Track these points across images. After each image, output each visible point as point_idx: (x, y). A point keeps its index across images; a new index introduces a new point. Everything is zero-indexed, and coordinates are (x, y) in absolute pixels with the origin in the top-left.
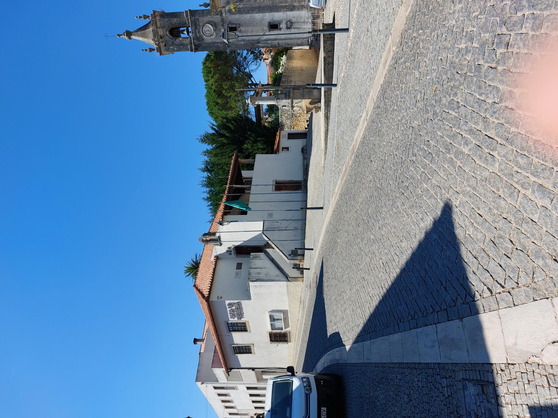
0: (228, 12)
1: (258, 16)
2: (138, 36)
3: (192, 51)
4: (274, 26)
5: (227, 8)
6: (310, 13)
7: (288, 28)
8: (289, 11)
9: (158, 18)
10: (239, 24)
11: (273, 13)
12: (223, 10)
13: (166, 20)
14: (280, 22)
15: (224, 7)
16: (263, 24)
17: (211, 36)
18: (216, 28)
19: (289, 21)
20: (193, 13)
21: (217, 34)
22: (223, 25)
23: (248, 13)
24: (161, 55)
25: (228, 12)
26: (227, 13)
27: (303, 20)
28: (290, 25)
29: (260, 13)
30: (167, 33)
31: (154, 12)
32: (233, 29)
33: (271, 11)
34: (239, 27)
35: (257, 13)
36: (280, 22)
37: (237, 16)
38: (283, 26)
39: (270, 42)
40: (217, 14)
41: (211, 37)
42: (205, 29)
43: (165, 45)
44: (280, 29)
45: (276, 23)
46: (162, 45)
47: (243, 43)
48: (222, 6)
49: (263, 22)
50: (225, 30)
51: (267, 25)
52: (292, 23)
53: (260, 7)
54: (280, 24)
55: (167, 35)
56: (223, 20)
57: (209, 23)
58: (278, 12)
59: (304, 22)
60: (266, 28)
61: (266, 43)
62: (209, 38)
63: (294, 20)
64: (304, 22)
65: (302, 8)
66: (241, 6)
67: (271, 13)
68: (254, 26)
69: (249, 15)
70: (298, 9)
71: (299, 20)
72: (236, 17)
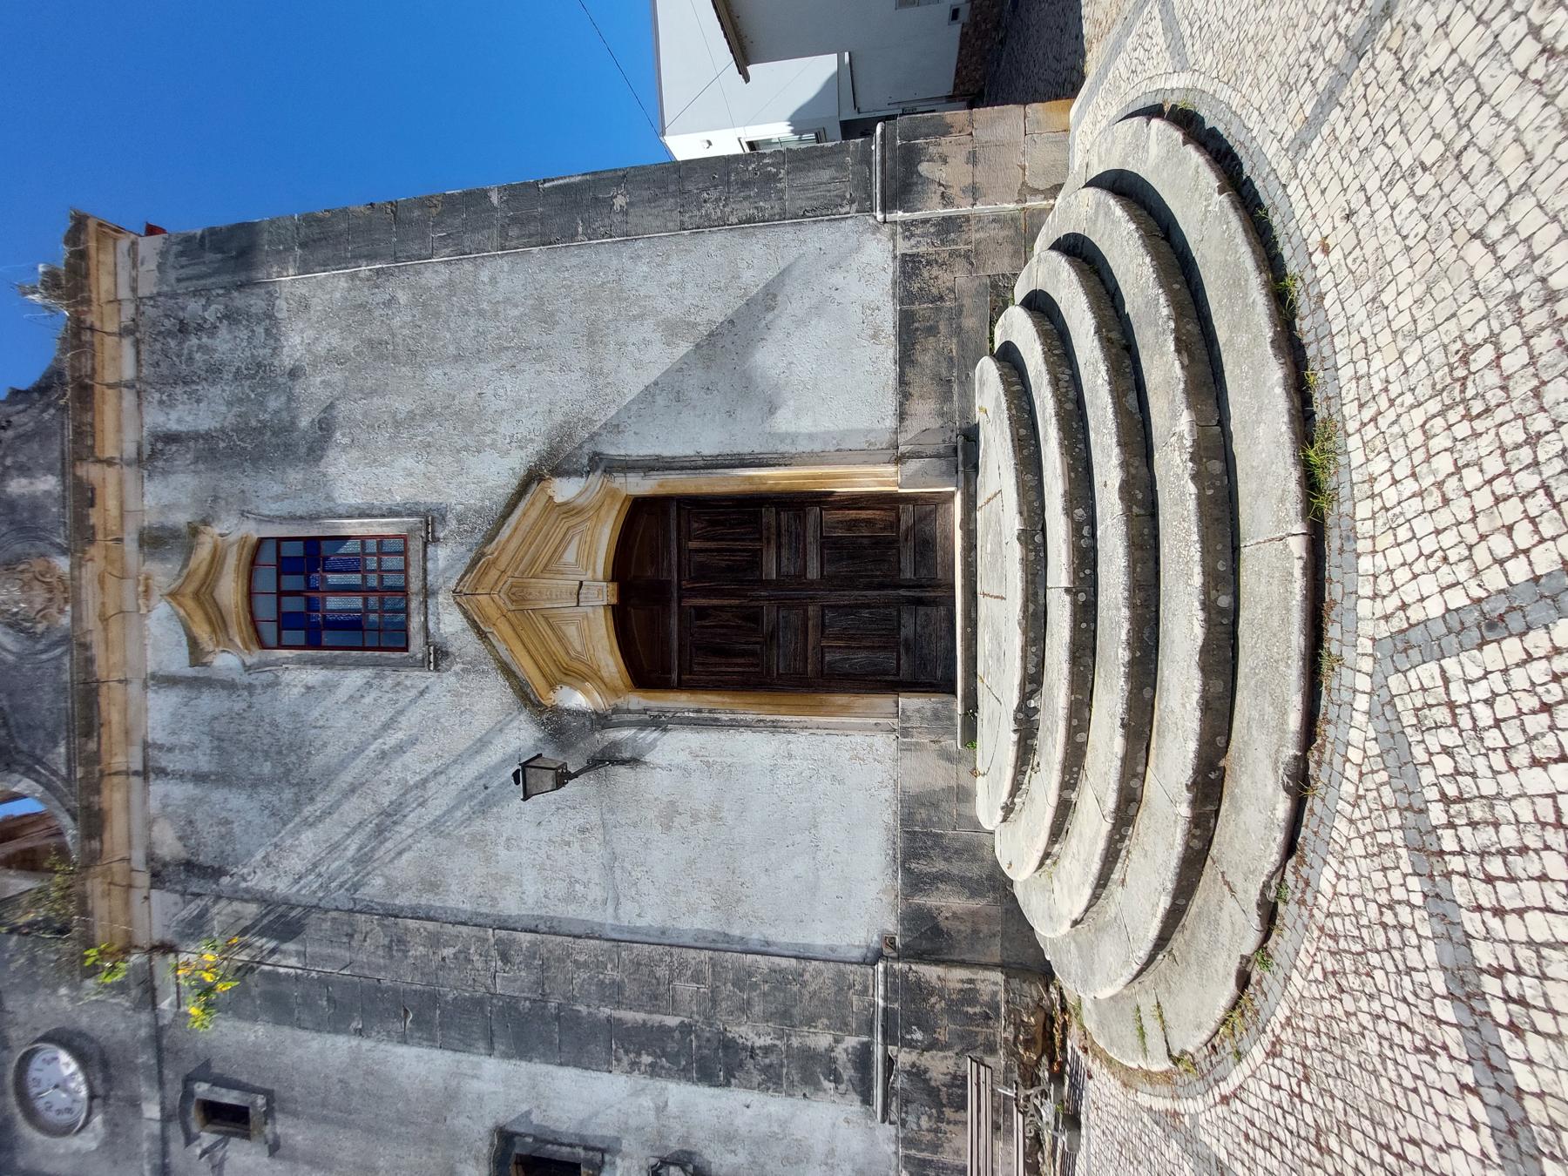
1: (415, 1064)
8: (683, 1074)
10: (269, 1095)
11: (538, 1068)
15: (166, 948)
16: (454, 1139)
17: (66, 1130)
18: (107, 1079)
21: (110, 1123)
23: (337, 1024)
29: (431, 1042)
33: (522, 1048)
34: (269, 1114)
35: (404, 1040)
48: (158, 935)
49: (460, 1122)
50: (166, 1119)
51: (485, 1149)
53: (434, 999)
57: (66, 1039)
66: (288, 962)
68: (374, 1131)
70: (772, 1080)
72: (241, 1040)
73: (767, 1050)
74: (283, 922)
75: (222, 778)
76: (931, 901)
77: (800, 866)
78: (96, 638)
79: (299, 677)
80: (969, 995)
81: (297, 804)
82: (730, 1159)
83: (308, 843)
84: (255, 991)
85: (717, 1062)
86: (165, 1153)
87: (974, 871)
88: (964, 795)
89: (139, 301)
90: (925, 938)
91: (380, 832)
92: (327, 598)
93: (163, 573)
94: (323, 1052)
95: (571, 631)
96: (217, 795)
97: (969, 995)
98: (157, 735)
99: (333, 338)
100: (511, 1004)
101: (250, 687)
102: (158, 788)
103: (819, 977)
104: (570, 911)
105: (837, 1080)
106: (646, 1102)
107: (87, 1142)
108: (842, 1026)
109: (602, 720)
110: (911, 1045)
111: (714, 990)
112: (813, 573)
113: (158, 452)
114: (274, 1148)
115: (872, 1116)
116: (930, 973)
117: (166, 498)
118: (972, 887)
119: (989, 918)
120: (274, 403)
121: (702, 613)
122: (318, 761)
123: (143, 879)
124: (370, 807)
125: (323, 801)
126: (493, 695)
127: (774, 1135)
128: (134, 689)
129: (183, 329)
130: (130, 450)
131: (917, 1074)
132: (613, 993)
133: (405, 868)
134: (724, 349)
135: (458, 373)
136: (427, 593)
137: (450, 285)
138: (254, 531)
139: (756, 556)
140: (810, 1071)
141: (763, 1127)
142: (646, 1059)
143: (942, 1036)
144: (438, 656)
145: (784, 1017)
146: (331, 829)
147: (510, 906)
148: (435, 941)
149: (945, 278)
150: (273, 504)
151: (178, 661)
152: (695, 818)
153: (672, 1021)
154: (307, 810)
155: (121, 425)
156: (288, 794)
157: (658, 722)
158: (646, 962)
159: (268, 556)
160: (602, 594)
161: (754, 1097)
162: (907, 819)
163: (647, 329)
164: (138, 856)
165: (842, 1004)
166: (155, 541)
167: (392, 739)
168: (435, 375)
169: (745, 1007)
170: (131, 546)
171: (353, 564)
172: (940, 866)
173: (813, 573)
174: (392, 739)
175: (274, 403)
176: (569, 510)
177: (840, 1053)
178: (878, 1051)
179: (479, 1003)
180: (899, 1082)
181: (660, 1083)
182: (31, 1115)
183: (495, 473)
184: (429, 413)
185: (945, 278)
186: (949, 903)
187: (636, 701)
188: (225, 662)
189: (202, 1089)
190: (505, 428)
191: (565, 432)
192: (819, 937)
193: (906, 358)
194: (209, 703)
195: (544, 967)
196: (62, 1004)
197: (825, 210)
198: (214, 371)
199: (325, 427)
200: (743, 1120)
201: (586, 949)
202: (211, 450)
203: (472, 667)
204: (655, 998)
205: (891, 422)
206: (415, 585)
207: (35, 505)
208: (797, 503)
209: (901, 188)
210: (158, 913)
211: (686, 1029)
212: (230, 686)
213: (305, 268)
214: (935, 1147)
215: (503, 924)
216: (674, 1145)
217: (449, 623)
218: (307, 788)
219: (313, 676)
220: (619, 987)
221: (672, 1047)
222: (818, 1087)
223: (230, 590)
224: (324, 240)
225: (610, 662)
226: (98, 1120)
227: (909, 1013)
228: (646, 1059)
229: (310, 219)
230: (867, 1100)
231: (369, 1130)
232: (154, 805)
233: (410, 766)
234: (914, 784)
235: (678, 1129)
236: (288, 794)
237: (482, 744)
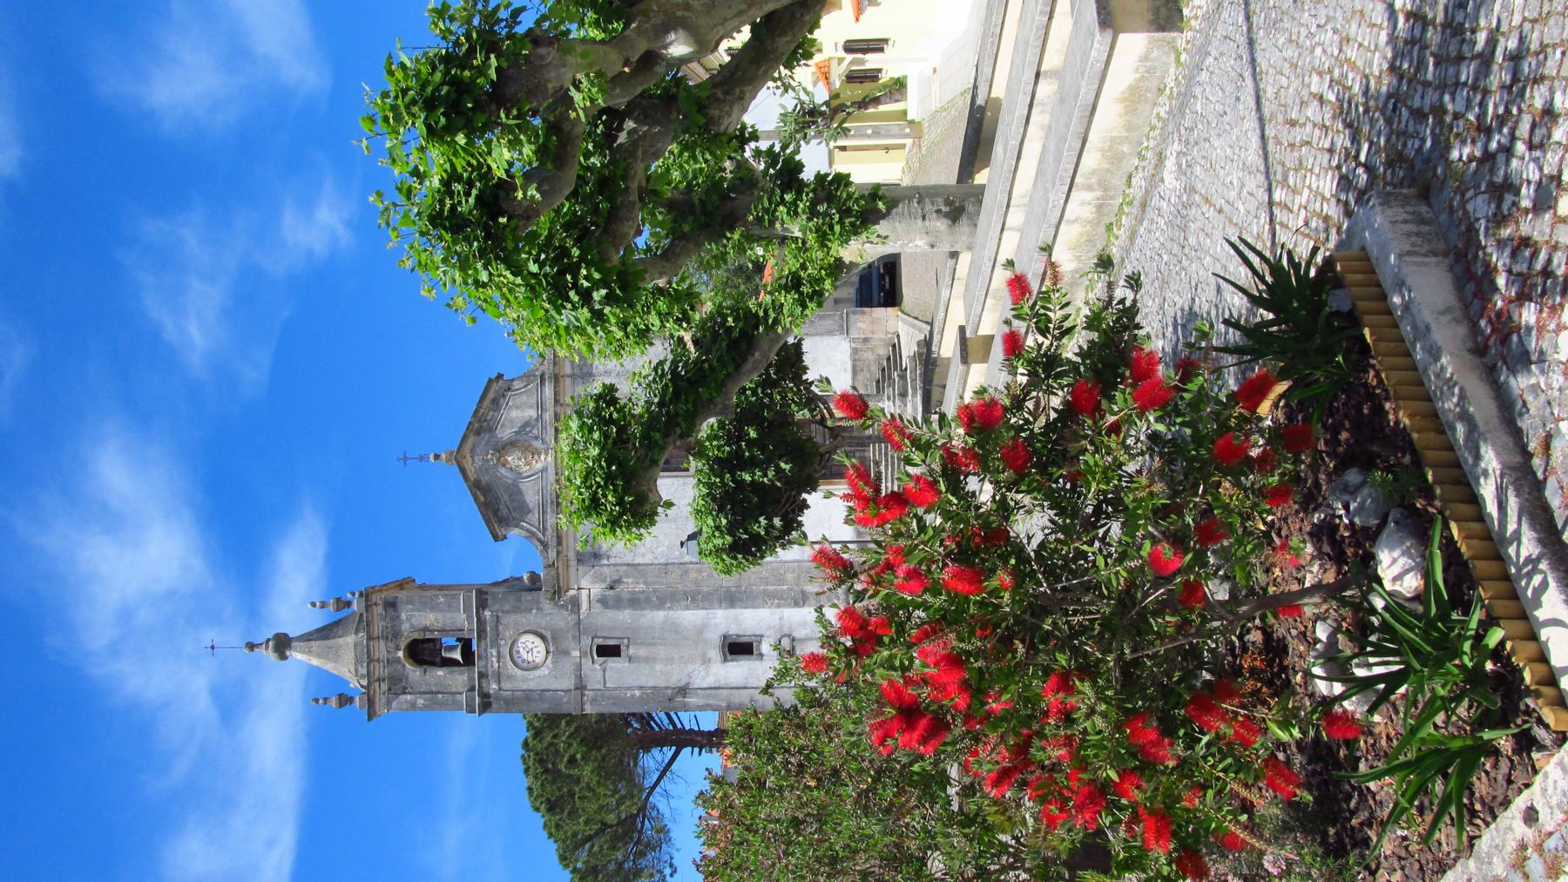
0: (599, 601)
1: (690, 617)
2: (310, 652)
3: (471, 710)
8: (789, 606)
17: (536, 667)
20: (483, 597)
23: (660, 605)
25: (599, 601)
29: (697, 607)
30: (401, 654)
35: (687, 608)
37: (625, 616)
41: (537, 673)
44: (761, 655)
45: (744, 640)
58: (753, 607)
60: (715, 654)
62: (532, 674)
63: (797, 634)
67: (732, 612)
94: (656, 617)
100: (728, 591)
106: (777, 617)
107: (545, 671)
114: (630, 659)
123: (573, 563)
164: (572, 555)
189: (600, 641)
196: (532, 619)
197: (830, 333)
204: (781, 581)
216: (786, 631)
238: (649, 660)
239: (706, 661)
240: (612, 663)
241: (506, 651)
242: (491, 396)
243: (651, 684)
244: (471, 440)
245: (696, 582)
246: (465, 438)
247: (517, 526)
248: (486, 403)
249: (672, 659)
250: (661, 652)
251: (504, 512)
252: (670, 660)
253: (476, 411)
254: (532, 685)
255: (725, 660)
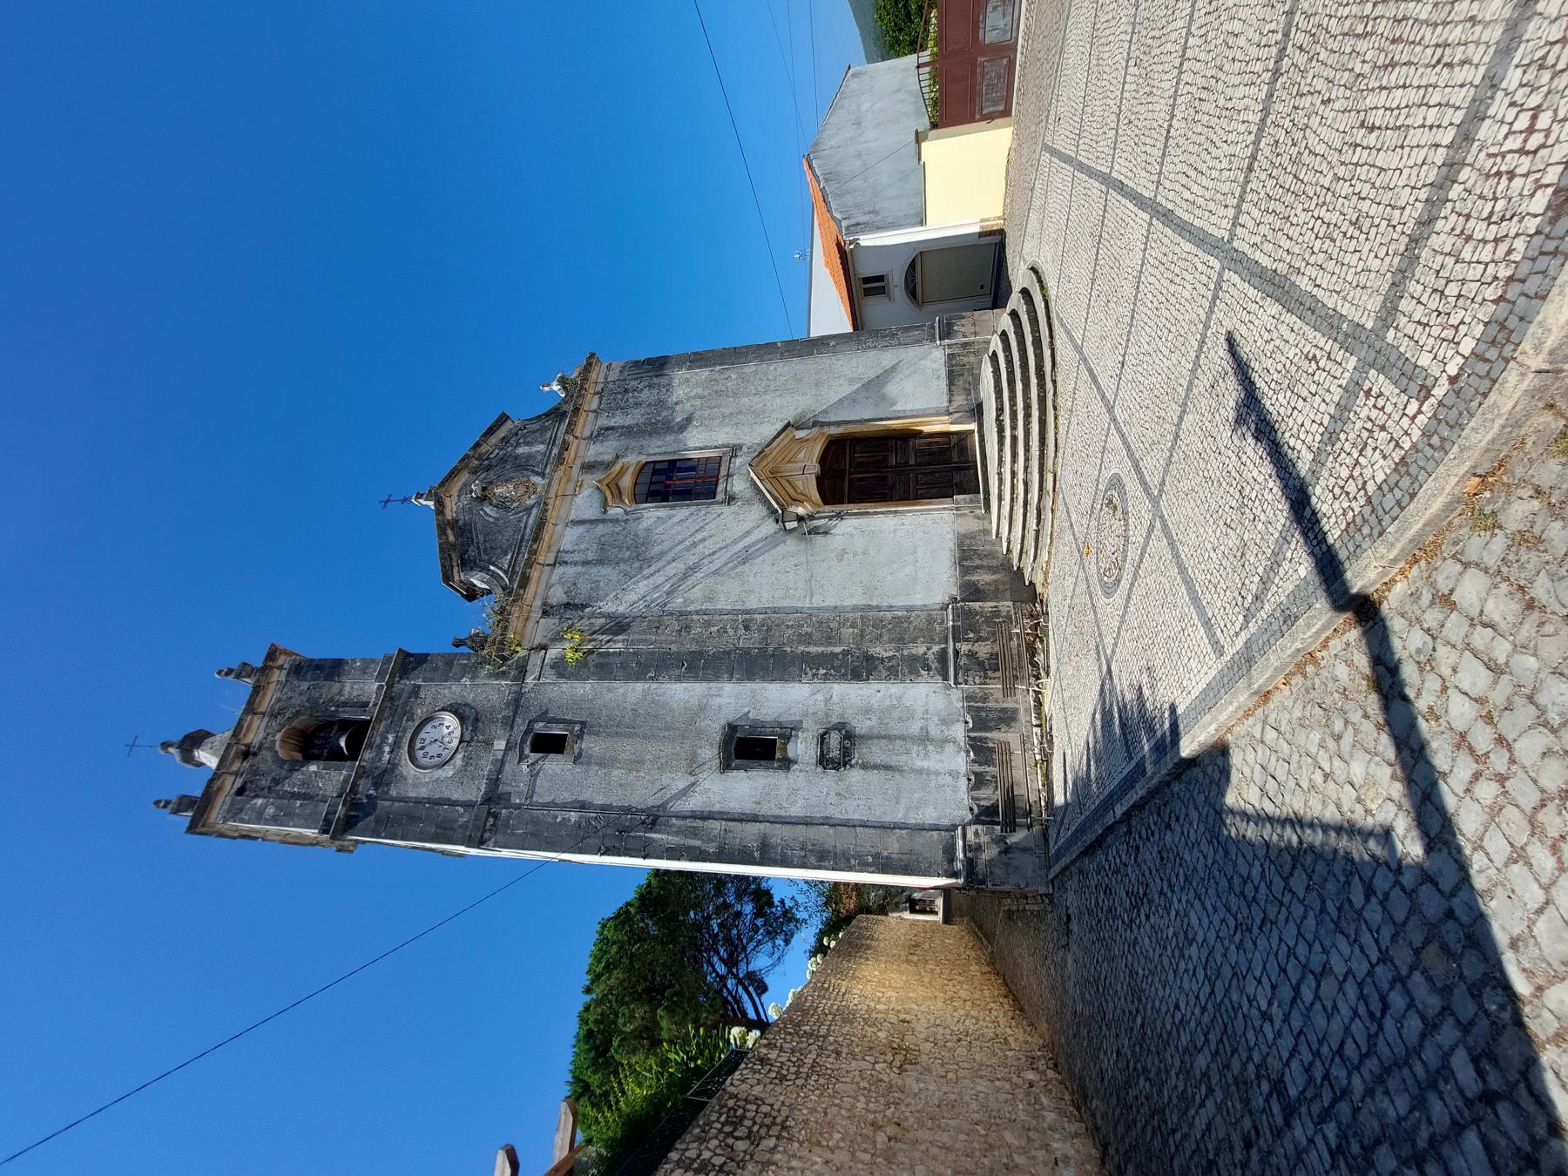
1: (680, 693)
4: (752, 747)
5: (553, 653)
6: (956, 694)
7: (824, 761)
8: (843, 678)
9: (278, 676)
10: (583, 724)
12: (536, 659)
13: (305, 685)
14: (788, 732)
16: (700, 733)
18: (475, 730)
19: (840, 727)
20: (408, 663)
21: (468, 760)
22: (510, 723)
23: (639, 676)
24: (192, 828)
25: (552, 667)
26: (548, 671)
27: (915, 728)
28: (841, 749)
29: (697, 679)
30: (278, 736)
31: (272, 654)
32: (549, 745)
33: (749, 676)
34: (580, 736)
35: (679, 679)
36: (788, 732)
38: (803, 748)
39: (716, 826)
40: (504, 675)
41: (440, 773)
42: (428, 733)
43: (241, 791)
44: (787, 764)
46: (230, 784)
47: (573, 816)
49: (703, 724)
50: (508, 748)
51: (717, 738)
52: (849, 736)
54: (788, 738)
55: (271, 748)
56: (517, 702)
57: (455, 710)
58: (781, 679)
59: (924, 739)
60: (709, 753)
61: (694, 833)
62: (426, 776)
63: (861, 726)
64: (924, 739)
65: (914, 672)
66: (618, 646)
69: (639, 687)
70: (893, 674)
71: (896, 728)
73: (890, 658)
74: (618, 626)
75: (600, 562)
76: (974, 578)
77: (907, 570)
78: (551, 502)
79: (652, 514)
80: (996, 613)
81: (641, 569)
82: (868, 723)
83: (643, 587)
84: (591, 664)
85: (861, 668)
86: (500, 771)
87: (995, 563)
88: (987, 532)
89: (606, 382)
90: (972, 592)
91: (685, 577)
92: (680, 482)
93: (591, 480)
94: (633, 691)
95: (799, 483)
96: (594, 570)
97: (996, 613)
98: (568, 547)
99: (700, 391)
100: (747, 651)
101: (626, 521)
102: (559, 570)
103: (919, 620)
104: (786, 603)
105: (929, 669)
106: (820, 697)
107: (448, 771)
108: (932, 641)
109: (811, 517)
110: (967, 640)
111: (862, 631)
112: (912, 462)
113: (601, 434)
114: (577, 759)
115: (949, 687)
116: (976, 605)
117: (602, 451)
118: (994, 570)
119: (1003, 583)
120: (664, 413)
121: (860, 480)
122: (656, 549)
123: (537, 614)
124: (682, 566)
125: (653, 568)
126: (757, 511)
127: (893, 706)
128: (559, 528)
129: (626, 391)
130: (587, 433)
131: (972, 655)
132: (807, 639)
133: (697, 593)
134: (875, 386)
135: (756, 399)
136: (729, 475)
137: (756, 372)
138: (644, 459)
139: (885, 459)
140: (913, 667)
141: (888, 703)
142: (822, 671)
143: (983, 634)
144: (731, 499)
145: (900, 640)
146: (659, 578)
147: (753, 603)
148: (708, 624)
149: (965, 359)
150: (658, 449)
151: (592, 512)
152: (855, 554)
153: (838, 650)
154: (646, 572)
155: (586, 425)
156: (637, 565)
157: (839, 516)
158: (825, 626)
159: (649, 469)
160: (814, 468)
161: (883, 686)
162: (960, 545)
163: (841, 381)
164: (538, 603)
165: (931, 630)
166: (588, 467)
167: (699, 536)
168: (745, 400)
169: (879, 638)
170: (576, 469)
171: (693, 469)
172: (978, 562)
173: (912, 462)
174: (699, 536)
175: (664, 413)
176: (801, 440)
177: (930, 655)
178: (951, 651)
179: (729, 653)
180: (963, 661)
181: (828, 685)
182: (413, 759)
183: (768, 430)
184: (741, 412)
185: (965, 359)
186: (983, 578)
187: (828, 508)
188: (615, 511)
189: (539, 727)
190: (774, 415)
191: (803, 414)
192: (918, 600)
193: (951, 383)
194: (601, 529)
195: (769, 630)
196: (456, 690)
197: (918, 342)
198: (637, 404)
199: (688, 420)
200: (875, 701)
201: (791, 620)
202: (628, 432)
203: (748, 502)
205: (945, 398)
206: (723, 472)
207: (530, 456)
208: (906, 437)
209: (947, 332)
210: (541, 629)
211: (845, 653)
212: (615, 521)
213: (690, 368)
214: (985, 699)
215: (748, 612)
216: (835, 720)
217: (738, 486)
218: (648, 561)
219: (662, 513)
220: (810, 635)
221: (837, 663)
222: (918, 675)
223: (627, 482)
224: (699, 359)
225: (816, 496)
226: (459, 756)
227: (967, 625)
228: (822, 671)
229: (695, 354)
230: (945, 678)
231: (645, 737)
232: (554, 578)
233: (710, 546)
234: (963, 530)
235: (838, 710)
236: (637, 565)
237: (748, 533)
238: (605, 762)
239: (693, 766)
240: (554, 765)
241: (409, 736)
242: (501, 433)
243: (599, 800)
244: (465, 476)
245: (698, 640)
246: (453, 474)
247: (485, 569)
248: (494, 439)
249: (641, 762)
250: (627, 748)
251: (472, 552)
252: (636, 764)
253: (477, 445)
254: (424, 792)
255: (726, 766)
